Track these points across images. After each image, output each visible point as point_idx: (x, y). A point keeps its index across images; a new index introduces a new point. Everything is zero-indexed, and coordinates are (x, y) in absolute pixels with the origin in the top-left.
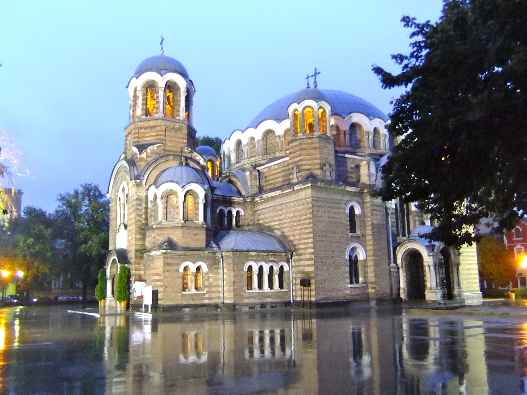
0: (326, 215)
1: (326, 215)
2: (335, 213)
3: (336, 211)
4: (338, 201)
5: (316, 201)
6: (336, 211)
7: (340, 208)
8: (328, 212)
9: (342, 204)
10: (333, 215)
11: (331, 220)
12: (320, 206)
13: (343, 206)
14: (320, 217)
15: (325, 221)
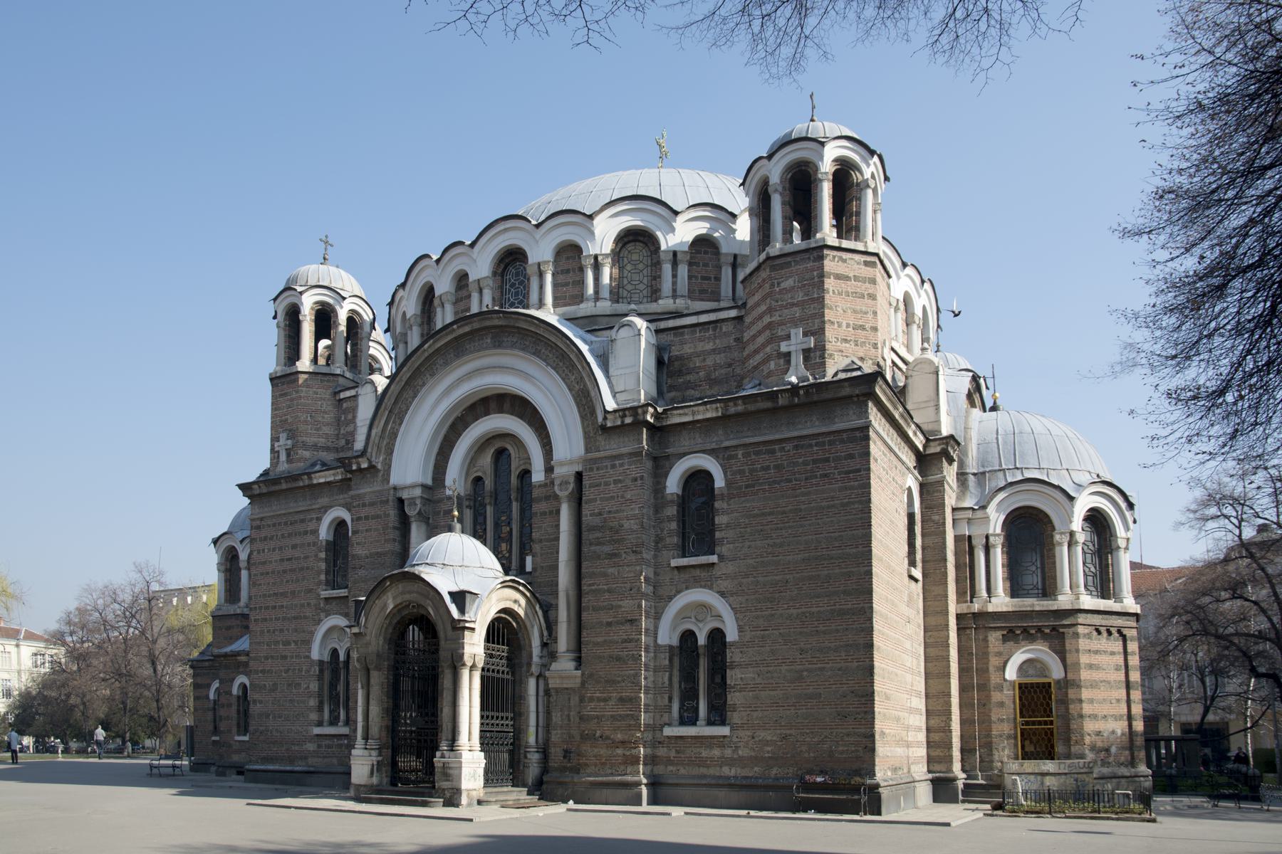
0: (276, 556)
1: (276, 556)
2: (294, 547)
3: (297, 540)
4: (302, 517)
5: (258, 528)
6: (297, 540)
7: (306, 533)
8: (281, 549)
9: (311, 519)
10: (289, 553)
11: (287, 565)
12: (265, 539)
13: (311, 526)
14: (264, 563)
15: (273, 572)
